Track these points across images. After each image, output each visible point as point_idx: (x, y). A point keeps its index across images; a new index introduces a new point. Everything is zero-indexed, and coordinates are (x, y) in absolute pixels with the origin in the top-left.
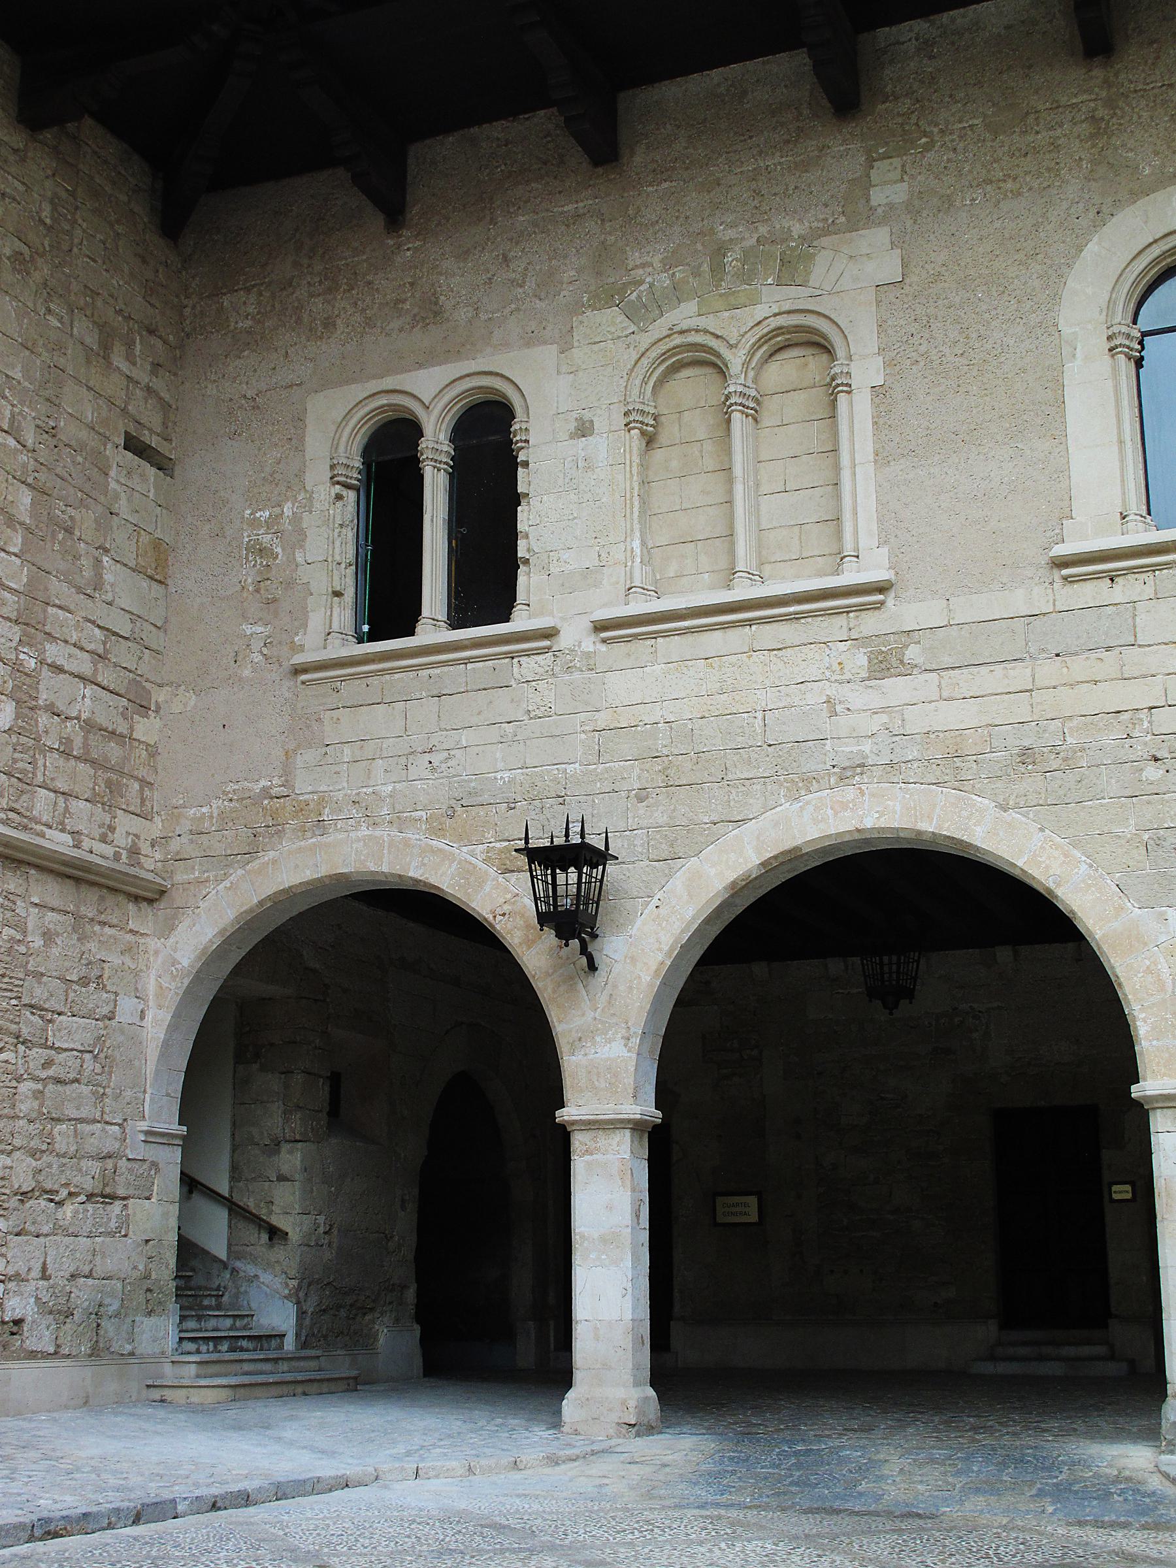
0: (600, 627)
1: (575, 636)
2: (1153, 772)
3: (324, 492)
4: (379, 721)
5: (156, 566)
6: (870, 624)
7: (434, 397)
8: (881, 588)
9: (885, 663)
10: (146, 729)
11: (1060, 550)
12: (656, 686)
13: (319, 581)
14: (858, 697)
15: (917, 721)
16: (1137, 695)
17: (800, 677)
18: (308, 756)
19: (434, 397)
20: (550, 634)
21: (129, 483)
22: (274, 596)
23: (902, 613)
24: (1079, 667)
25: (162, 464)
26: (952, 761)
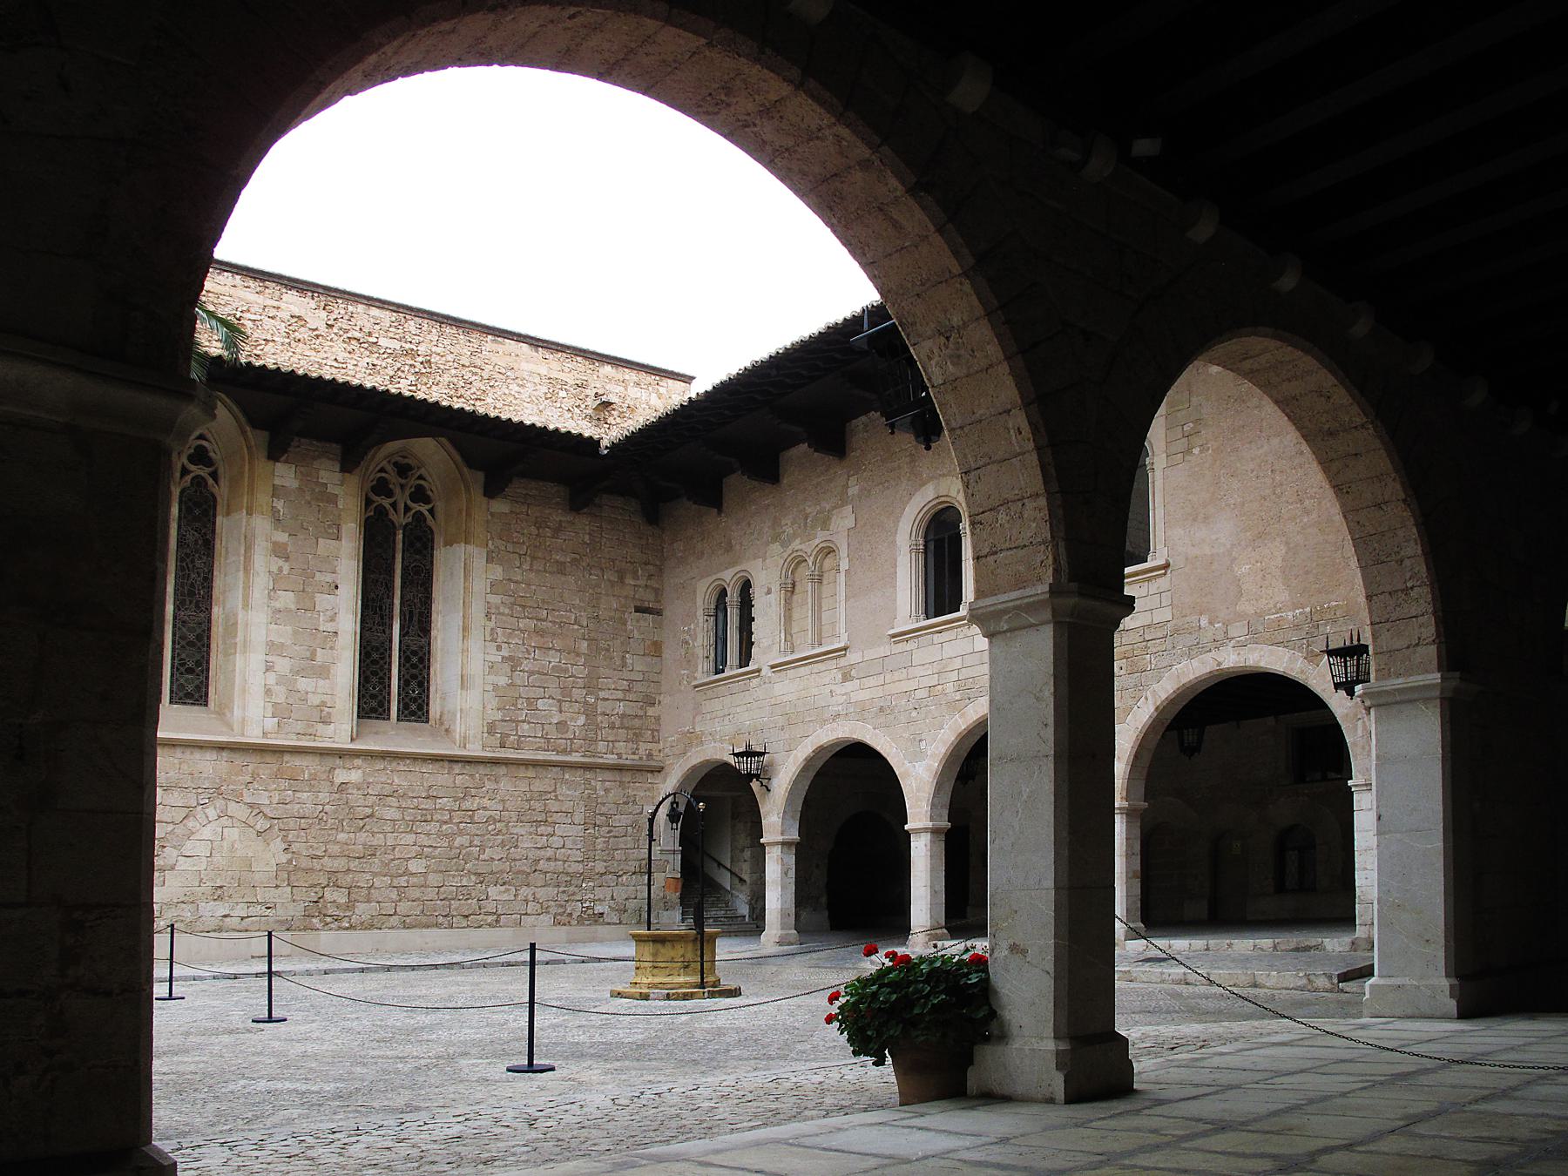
0: (772, 667)
1: (766, 671)
2: (914, 714)
3: (701, 618)
4: (716, 705)
5: (656, 649)
6: (843, 662)
7: (729, 577)
8: (845, 649)
9: (846, 677)
10: (651, 711)
11: (892, 632)
12: (786, 688)
13: (700, 653)
14: (839, 690)
15: (855, 697)
16: (912, 685)
17: (821, 684)
18: (699, 718)
19: (729, 577)
20: (759, 671)
21: (638, 625)
22: (689, 661)
23: (853, 657)
24: (897, 675)
25: (658, 613)
26: (861, 712)
